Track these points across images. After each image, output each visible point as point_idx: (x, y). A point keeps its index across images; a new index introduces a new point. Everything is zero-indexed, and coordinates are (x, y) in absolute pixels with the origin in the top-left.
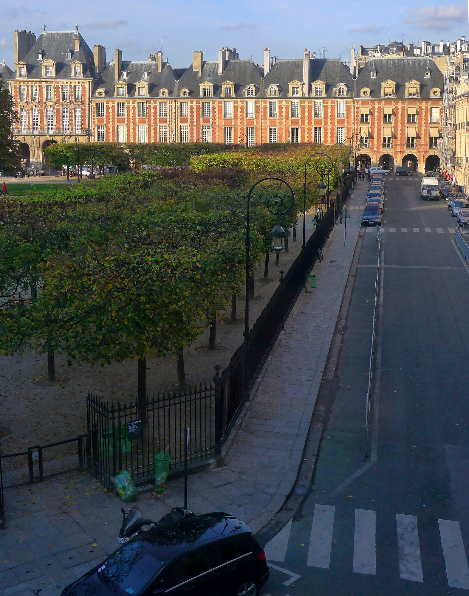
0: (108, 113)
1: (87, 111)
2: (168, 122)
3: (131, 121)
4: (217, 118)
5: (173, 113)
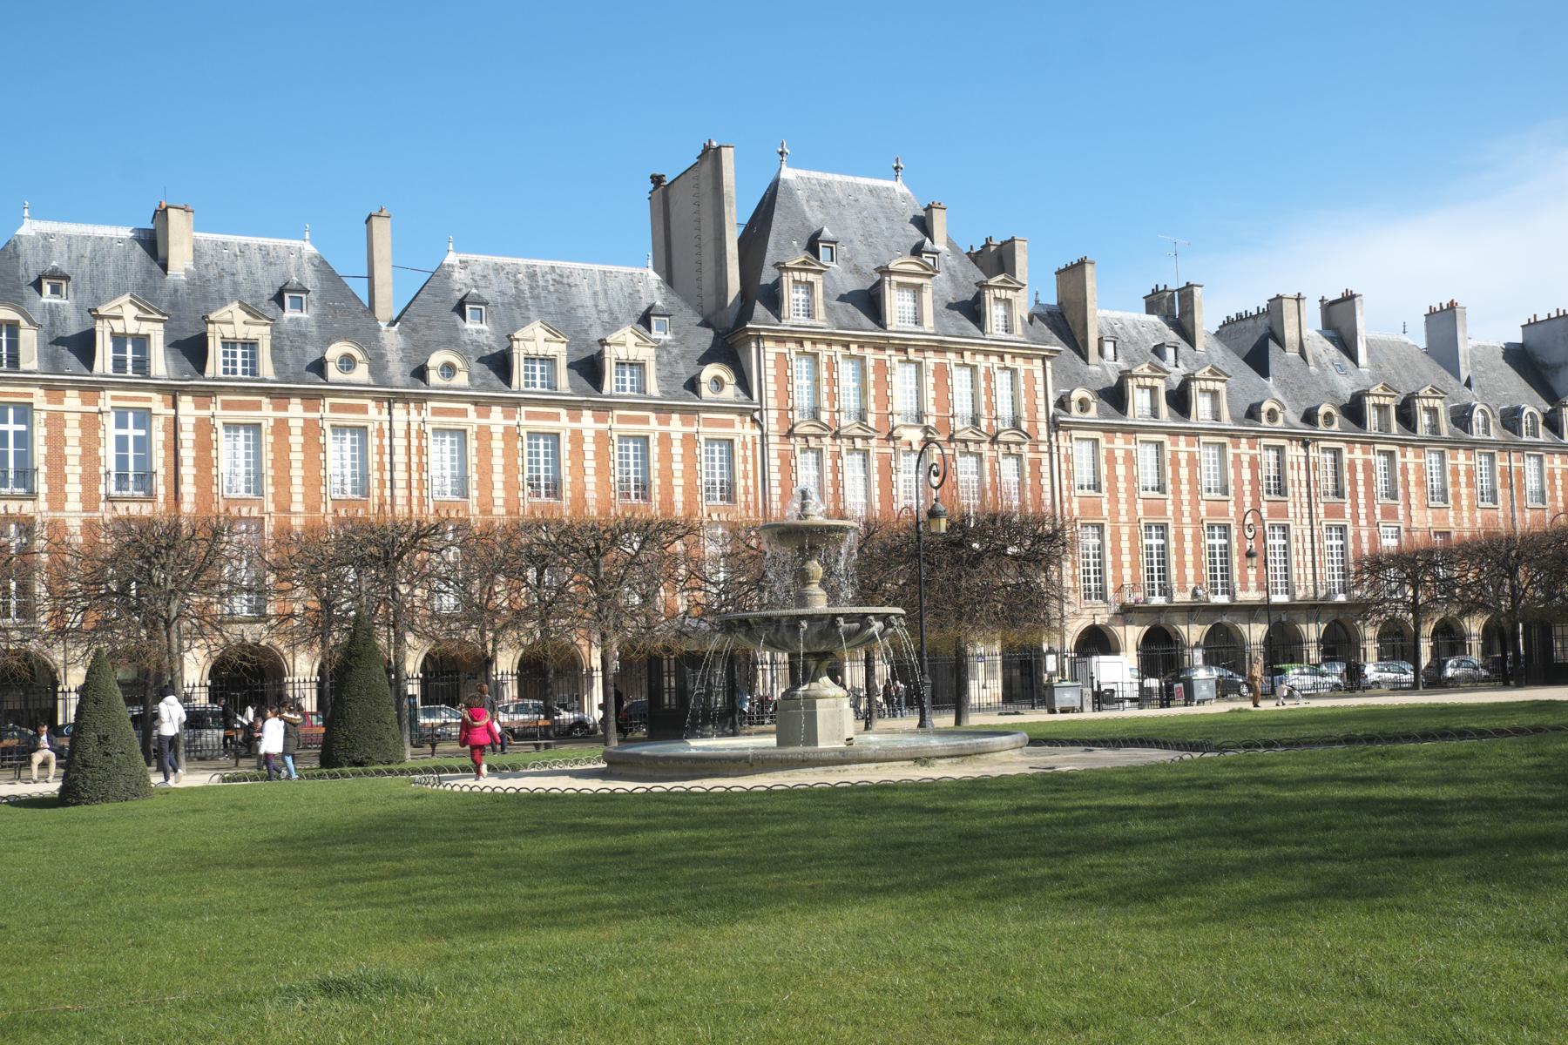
0: (1113, 478)
1: (1045, 469)
2: (1291, 515)
3: (1186, 508)
4: (1413, 501)
5: (1304, 484)
